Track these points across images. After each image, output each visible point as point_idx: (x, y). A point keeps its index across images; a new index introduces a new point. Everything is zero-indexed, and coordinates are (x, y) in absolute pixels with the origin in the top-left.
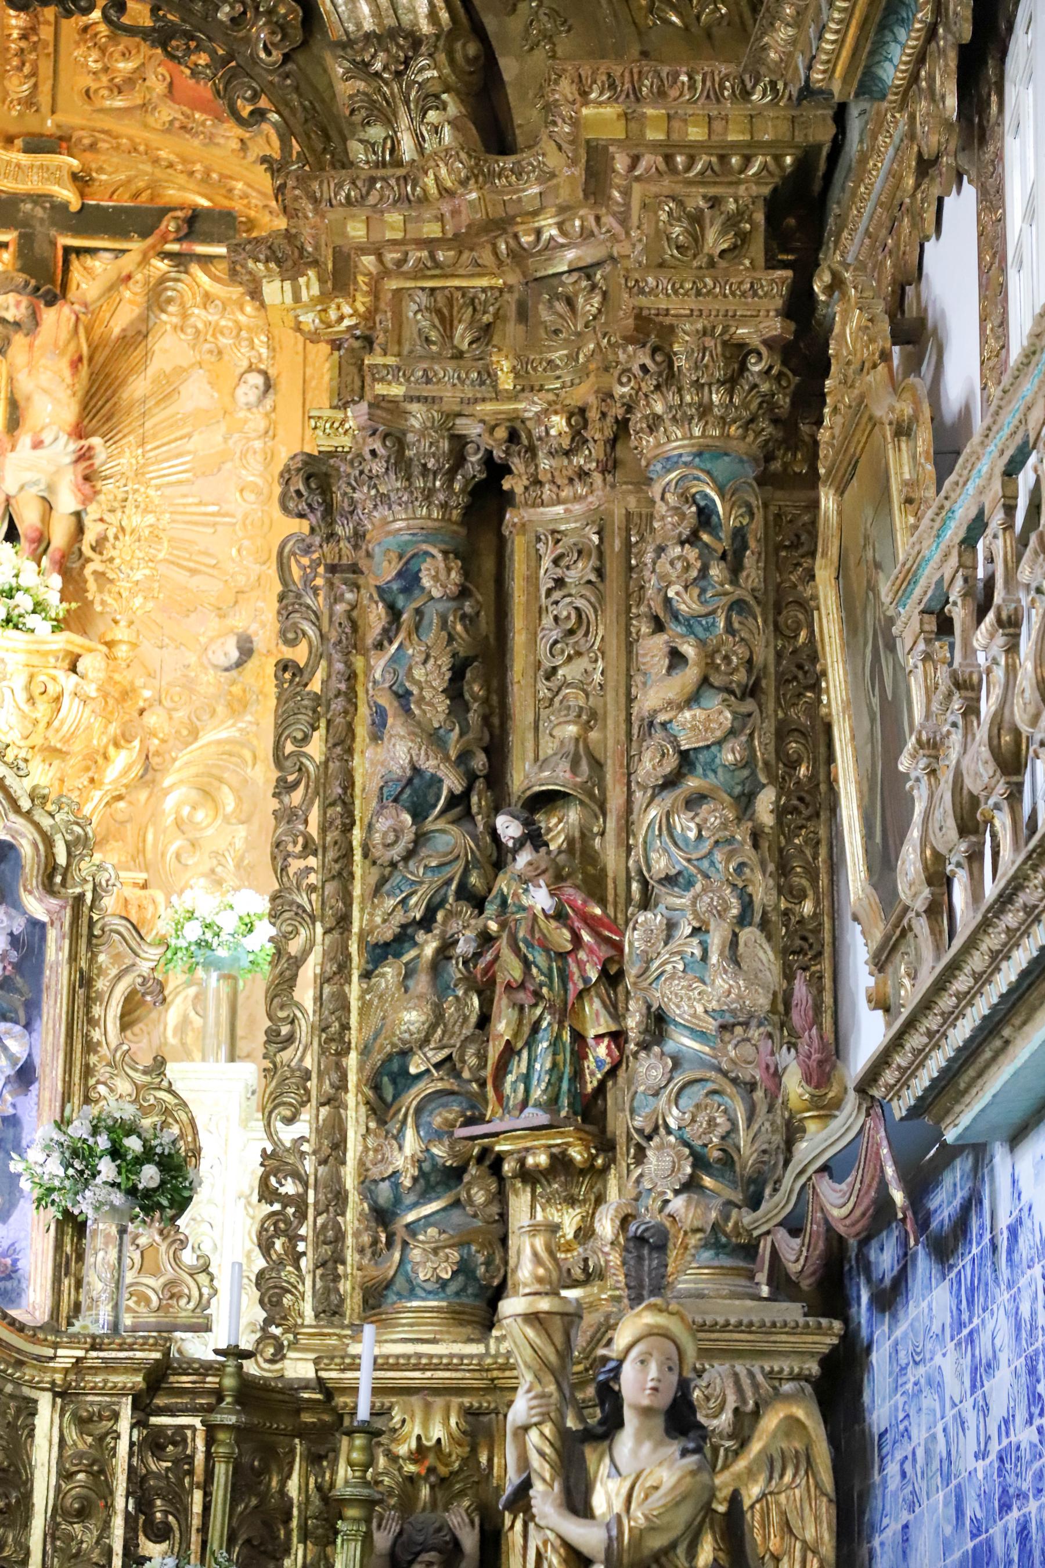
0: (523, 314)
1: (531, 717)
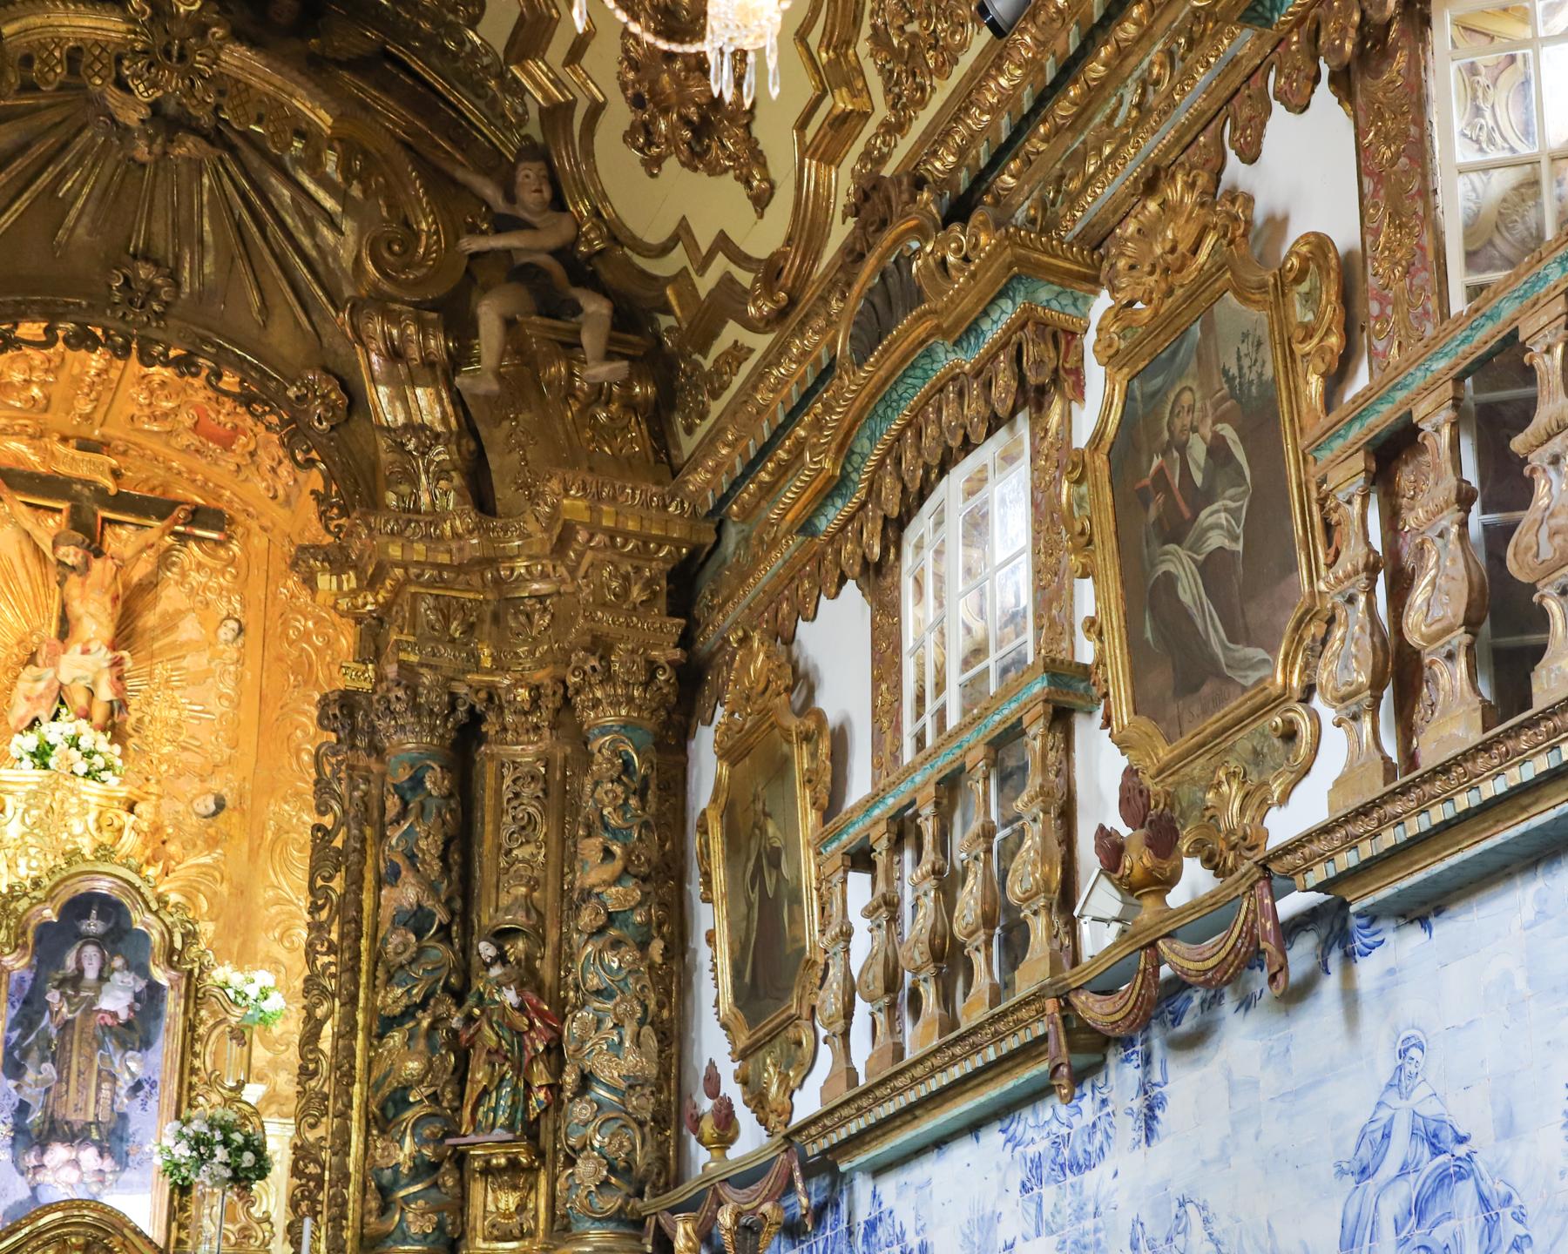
0: (496, 618)
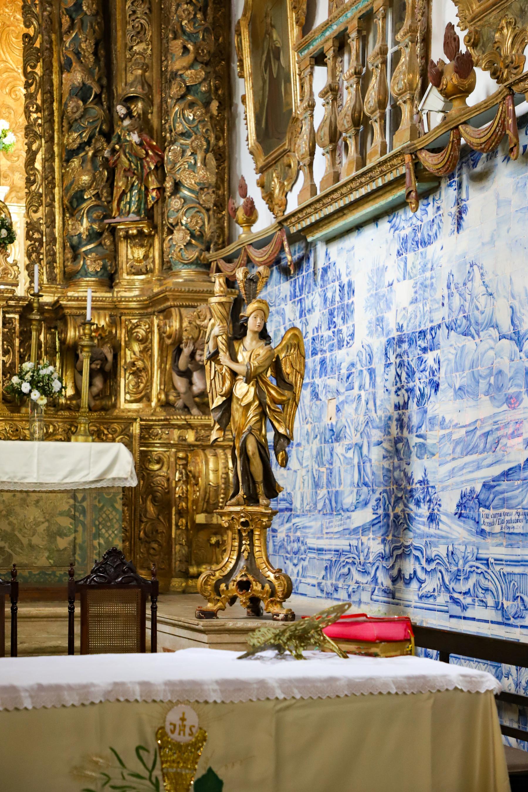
1: (124, 65)
